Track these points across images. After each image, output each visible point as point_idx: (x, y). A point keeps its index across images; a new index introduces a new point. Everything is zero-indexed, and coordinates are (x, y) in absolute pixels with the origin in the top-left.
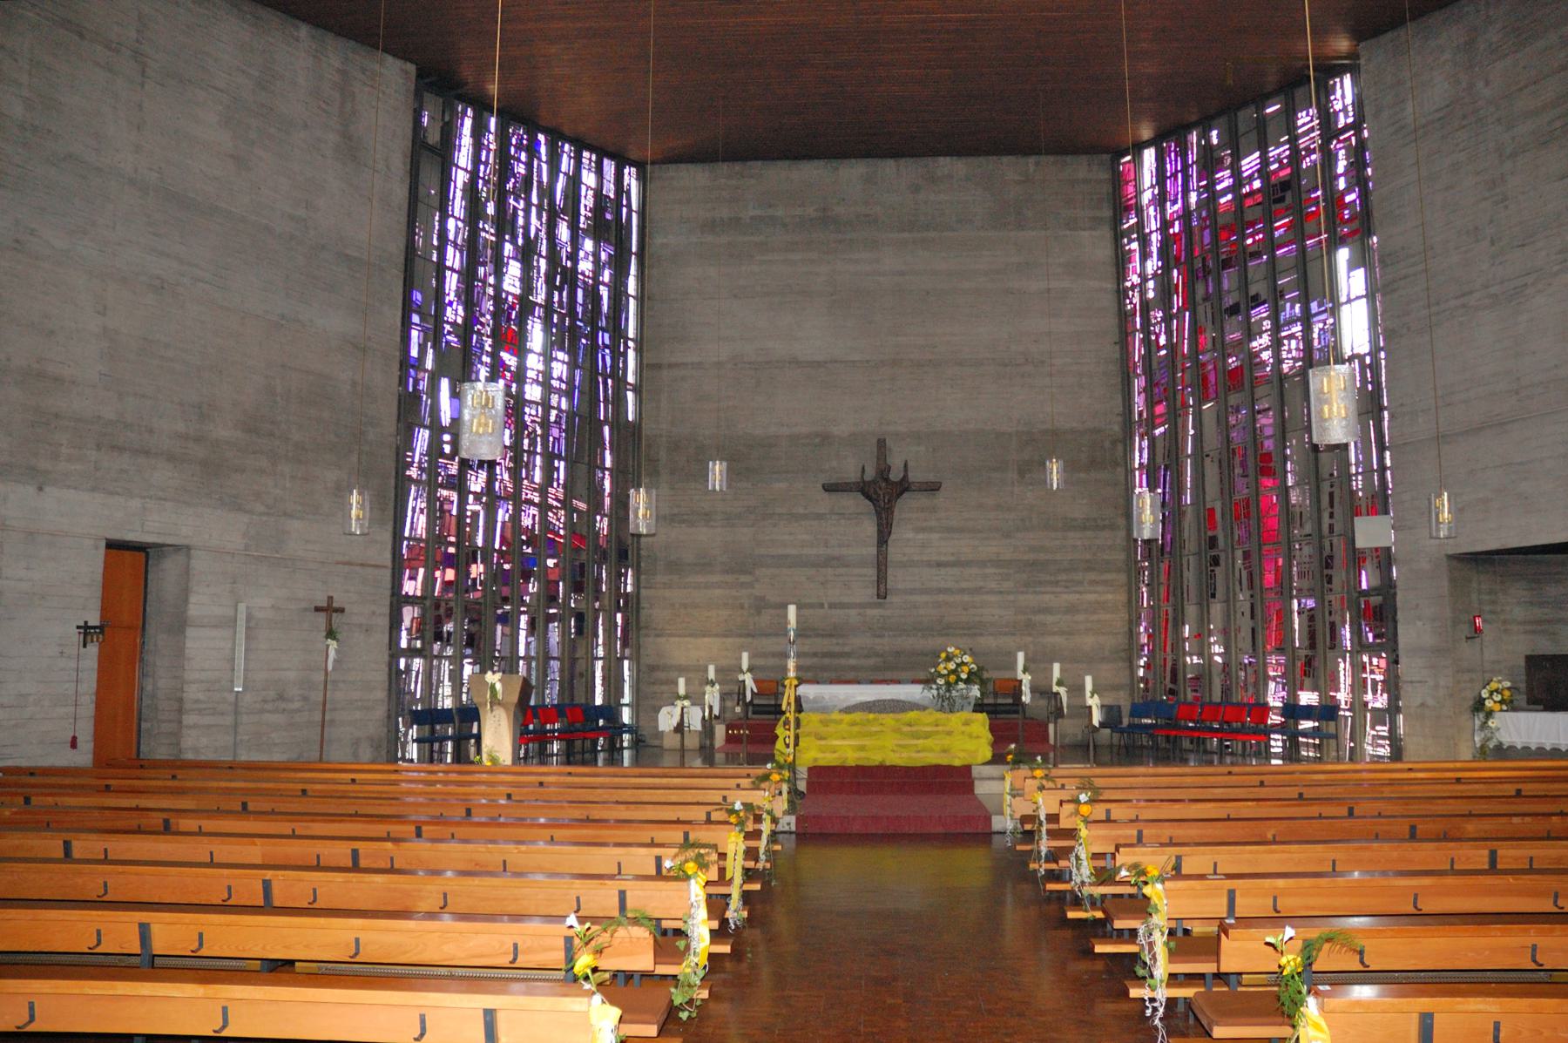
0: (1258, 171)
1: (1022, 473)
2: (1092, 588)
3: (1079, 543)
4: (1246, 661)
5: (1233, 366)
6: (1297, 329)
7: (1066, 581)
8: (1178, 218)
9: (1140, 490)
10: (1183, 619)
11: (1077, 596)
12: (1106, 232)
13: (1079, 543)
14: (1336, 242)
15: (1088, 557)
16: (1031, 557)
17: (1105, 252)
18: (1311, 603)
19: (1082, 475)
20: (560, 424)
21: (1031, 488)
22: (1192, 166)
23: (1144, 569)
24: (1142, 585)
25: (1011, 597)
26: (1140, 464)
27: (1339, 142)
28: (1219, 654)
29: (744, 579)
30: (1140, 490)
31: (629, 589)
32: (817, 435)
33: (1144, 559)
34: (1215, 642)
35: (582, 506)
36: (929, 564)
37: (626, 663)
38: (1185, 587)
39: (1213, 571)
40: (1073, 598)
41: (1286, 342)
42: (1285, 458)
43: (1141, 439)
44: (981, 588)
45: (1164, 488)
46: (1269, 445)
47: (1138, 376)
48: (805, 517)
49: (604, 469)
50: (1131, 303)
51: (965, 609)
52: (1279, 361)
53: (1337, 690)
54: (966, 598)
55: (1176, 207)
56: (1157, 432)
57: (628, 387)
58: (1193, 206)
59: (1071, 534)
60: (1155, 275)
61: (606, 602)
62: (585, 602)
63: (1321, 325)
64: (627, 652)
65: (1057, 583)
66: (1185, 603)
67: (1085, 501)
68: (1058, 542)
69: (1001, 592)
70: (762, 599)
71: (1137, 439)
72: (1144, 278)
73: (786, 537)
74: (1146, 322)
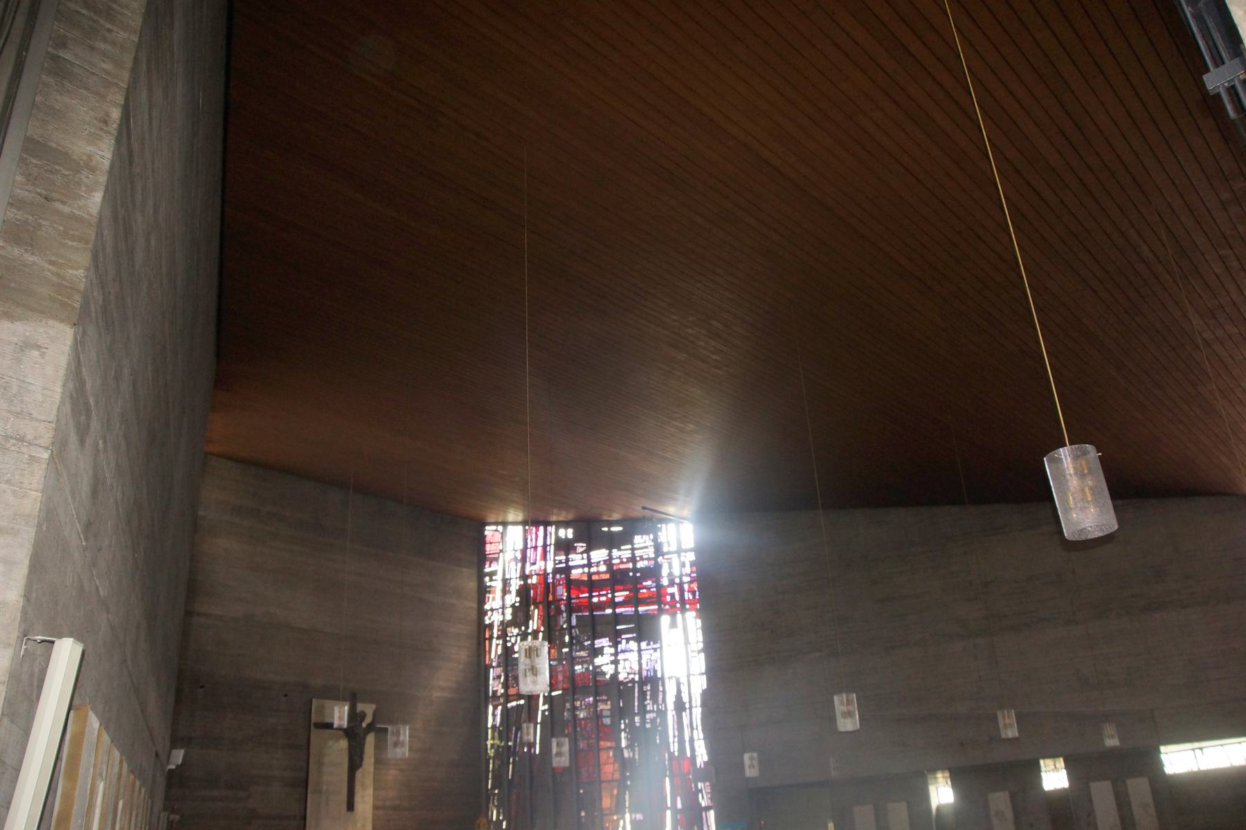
5: (578, 671)
6: (633, 656)
9: (492, 742)
12: (474, 571)
14: (661, 611)
17: (472, 585)
18: (639, 816)
23: (495, 794)
24: (491, 805)
26: (494, 727)
27: (664, 558)
30: (492, 742)
33: (494, 787)
41: (621, 662)
43: (495, 708)
47: (493, 667)
52: (616, 673)
55: (534, 568)
58: (549, 570)
60: (513, 606)
63: (649, 657)
71: (491, 708)
72: (503, 607)
74: (503, 635)
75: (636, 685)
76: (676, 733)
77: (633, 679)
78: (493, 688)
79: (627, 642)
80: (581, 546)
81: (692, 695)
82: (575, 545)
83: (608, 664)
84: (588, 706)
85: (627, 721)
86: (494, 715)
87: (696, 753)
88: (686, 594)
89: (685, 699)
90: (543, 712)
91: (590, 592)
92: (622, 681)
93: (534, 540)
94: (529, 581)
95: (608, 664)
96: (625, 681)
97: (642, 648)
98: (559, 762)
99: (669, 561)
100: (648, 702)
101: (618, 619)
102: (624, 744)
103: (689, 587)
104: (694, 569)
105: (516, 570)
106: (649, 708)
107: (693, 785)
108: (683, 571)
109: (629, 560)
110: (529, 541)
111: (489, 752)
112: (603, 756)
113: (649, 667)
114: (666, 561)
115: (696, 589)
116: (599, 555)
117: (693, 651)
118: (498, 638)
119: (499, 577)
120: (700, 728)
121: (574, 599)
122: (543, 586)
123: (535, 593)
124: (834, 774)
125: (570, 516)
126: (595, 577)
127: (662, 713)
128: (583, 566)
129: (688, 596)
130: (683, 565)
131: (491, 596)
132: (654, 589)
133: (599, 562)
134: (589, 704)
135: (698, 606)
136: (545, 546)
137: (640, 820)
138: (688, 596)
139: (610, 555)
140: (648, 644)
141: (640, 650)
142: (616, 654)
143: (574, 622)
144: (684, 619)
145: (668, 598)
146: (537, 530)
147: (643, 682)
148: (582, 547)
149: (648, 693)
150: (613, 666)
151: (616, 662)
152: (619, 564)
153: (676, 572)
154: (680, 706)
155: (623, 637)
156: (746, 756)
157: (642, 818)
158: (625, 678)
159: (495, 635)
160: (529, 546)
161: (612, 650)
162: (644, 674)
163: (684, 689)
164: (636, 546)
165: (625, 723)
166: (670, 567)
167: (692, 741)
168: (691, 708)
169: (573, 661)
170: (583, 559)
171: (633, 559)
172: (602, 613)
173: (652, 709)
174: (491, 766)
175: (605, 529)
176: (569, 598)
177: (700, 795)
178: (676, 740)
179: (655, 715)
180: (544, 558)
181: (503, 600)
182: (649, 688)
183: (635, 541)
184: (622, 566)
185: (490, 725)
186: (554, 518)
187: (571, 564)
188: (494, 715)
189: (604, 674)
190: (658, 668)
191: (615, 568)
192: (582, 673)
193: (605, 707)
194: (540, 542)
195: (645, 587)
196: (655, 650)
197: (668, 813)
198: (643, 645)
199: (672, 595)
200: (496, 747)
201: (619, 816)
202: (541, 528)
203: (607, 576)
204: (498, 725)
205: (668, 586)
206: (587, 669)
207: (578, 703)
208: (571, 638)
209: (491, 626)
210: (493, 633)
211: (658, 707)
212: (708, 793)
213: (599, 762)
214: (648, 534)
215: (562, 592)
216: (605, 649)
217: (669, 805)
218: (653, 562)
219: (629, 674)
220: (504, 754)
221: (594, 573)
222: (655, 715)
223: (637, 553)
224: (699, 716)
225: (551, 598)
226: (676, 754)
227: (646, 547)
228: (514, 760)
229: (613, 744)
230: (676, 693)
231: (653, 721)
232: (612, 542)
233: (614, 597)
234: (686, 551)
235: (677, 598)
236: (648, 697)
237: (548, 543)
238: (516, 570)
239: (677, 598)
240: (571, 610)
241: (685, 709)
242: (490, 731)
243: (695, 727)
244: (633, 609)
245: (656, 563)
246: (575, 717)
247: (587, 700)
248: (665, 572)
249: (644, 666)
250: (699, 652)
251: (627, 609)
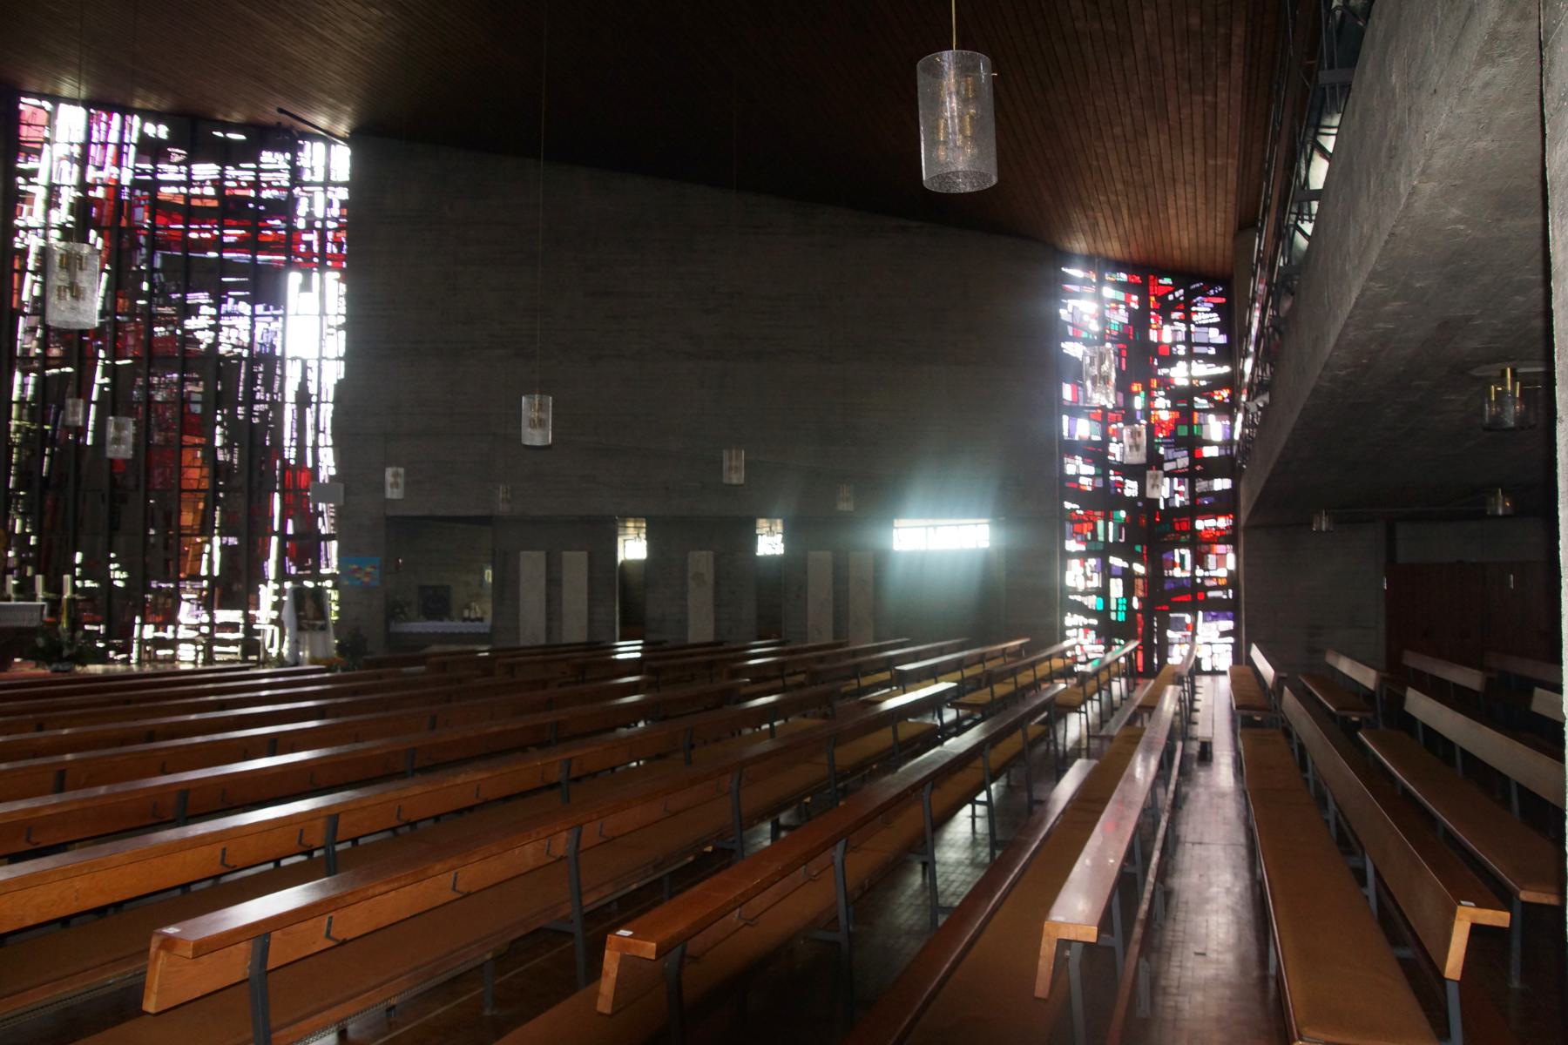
0: (213, 181)
5: (159, 334)
6: (243, 322)
8: (104, 185)
9: (17, 422)
14: (290, 265)
18: (233, 541)
22: (128, 145)
24: (12, 512)
26: (22, 401)
27: (303, 191)
30: (17, 422)
33: (18, 487)
34: (116, 570)
41: (224, 328)
42: (216, 424)
43: (25, 374)
46: (197, 409)
47: (25, 315)
50: (22, 243)
53: (257, 608)
55: (100, 174)
56: (48, 372)
63: (266, 326)
75: (243, 363)
76: (295, 435)
77: (240, 354)
79: (236, 303)
80: (177, 154)
81: (323, 386)
82: (169, 150)
83: (203, 329)
84: (167, 386)
85: (225, 412)
87: (320, 464)
88: (329, 245)
89: (313, 389)
90: (102, 386)
91: (187, 223)
92: (223, 355)
93: (103, 133)
94: (91, 193)
95: (203, 329)
96: (227, 355)
97: (257, 312)
98: (117, 451)
99: (309, 195)
100: (259, 387)
101: (224, 267)
102: (218, 442)
103: (335, 236)
104: (345, 212)
105: (71, 173)
106: (259, 396)
107: (311, 506)
108: (328, 213)
109: (251, 185)
110: (95, 133)
112: (187, 457)
113: (265, 340)
114: (304, 194)
115: (343, 240)
116: (205, 171)
117: (330, 327)
118: (34, 273)
119: (42, 179)
120: (329, 431)
121: (160, 229)
122: (112, 203)
123: (100, 214)
124: (503, 508)
125: (165, 105)
126: (196, 202)
127: (277, 407)
128: (178, 184)
129: (331, 248)
130: (329, 204)
131: (26, 207)
132: (283, 232)
133: (204, 181)
134: (171, 381)
135: (344, 265)
136: (120, 145)
137: (234, 546)
138: (331, 248)
139: (222, 174)
140: (267, 309)
141: (253, 316)
142: (217, 317)
143: (158, 263)
144: (322, 281)
145: (303, 248)
146: (110, 118)
147: (253, 360)
148: (180, 154)
149: (260, 376)
150: (212, 334)
151: (216, 329)
152: (233, 188)
153: (319, 212)
154: (303, 399)
155: (230, 293)
156: (389, 472)
157: (236, 543)
158: (229, 352)
159: (31, 267)
160: (94, 140)
161: (213, 311)
162: (257, 348)
163: (312, 375)
164: (262, 166)
165: (222, 414)
166: (311, 205)
167: (316, 447)
168: (318, 403)
169: (152, 319)
170: (180, 173)
171: (256, 185)
172: (202, 255)
173: (262, 398)
175: (219, 134)
176: (153, 227)
177: (320, 519)
178: (294, 444)
179: (266, 407)
180: (118, 163)
181: (47, 215)
182: (261, 369)
183: (262, 159)
184: (239, 192)
185: (15, 397)
186: (138, 104)
187: (160, 177)
189: (199, 342)
190: (278, 342)
191: (227, 192)
192: (164, 338)
193: (195, 389)
194: (114, 137)
195: (270, 228)
196: (276, 317)
197: (274, 540)
198: (260, 309)
199: (309, 244)
200: (23, 430)
201: (205, 538)
202: (117, 117)
203: (215, 204)
204: (28, 399)
205: (304, 231)
206: (173, 332)
207: (155, 380)
208: (152, 286)
209: (24, 253)
210: (26, 263)
211: (272, 397)
212: (332, 517)
213: (181, 462)
214: (283, 151)
215: (143, 217)
216: (202, 308)
217: (276, 528)
218: (285, 193)
219: (234, 346)
220: (35, 442)
221: (196, 197)
222: (266, 407)
223: (264, 177)
224: (329, 415)
225: (124, 223)
226: (292, 462)
227: (278, 171)
228: (52, 451)
229: (203, 440)
230: (299, 380)
231: (263, 414)
232: (227, 155)
233: (223, 235)
234: (336, 185)
235: (316, 249)
236: (259, 382)
237: (126, 140)
238: (71, 173)
239: (316, 249)
240: (154, 245)
241: (309, 404)
242: (15, 407)
243: (322, 429)
244: (249, 256)
245: (291, 195)
246: (149, 400)
247: (168, 376)
248: (302, 209)
249: (258, 338)
250: (339, 328)
251: (239, 255)
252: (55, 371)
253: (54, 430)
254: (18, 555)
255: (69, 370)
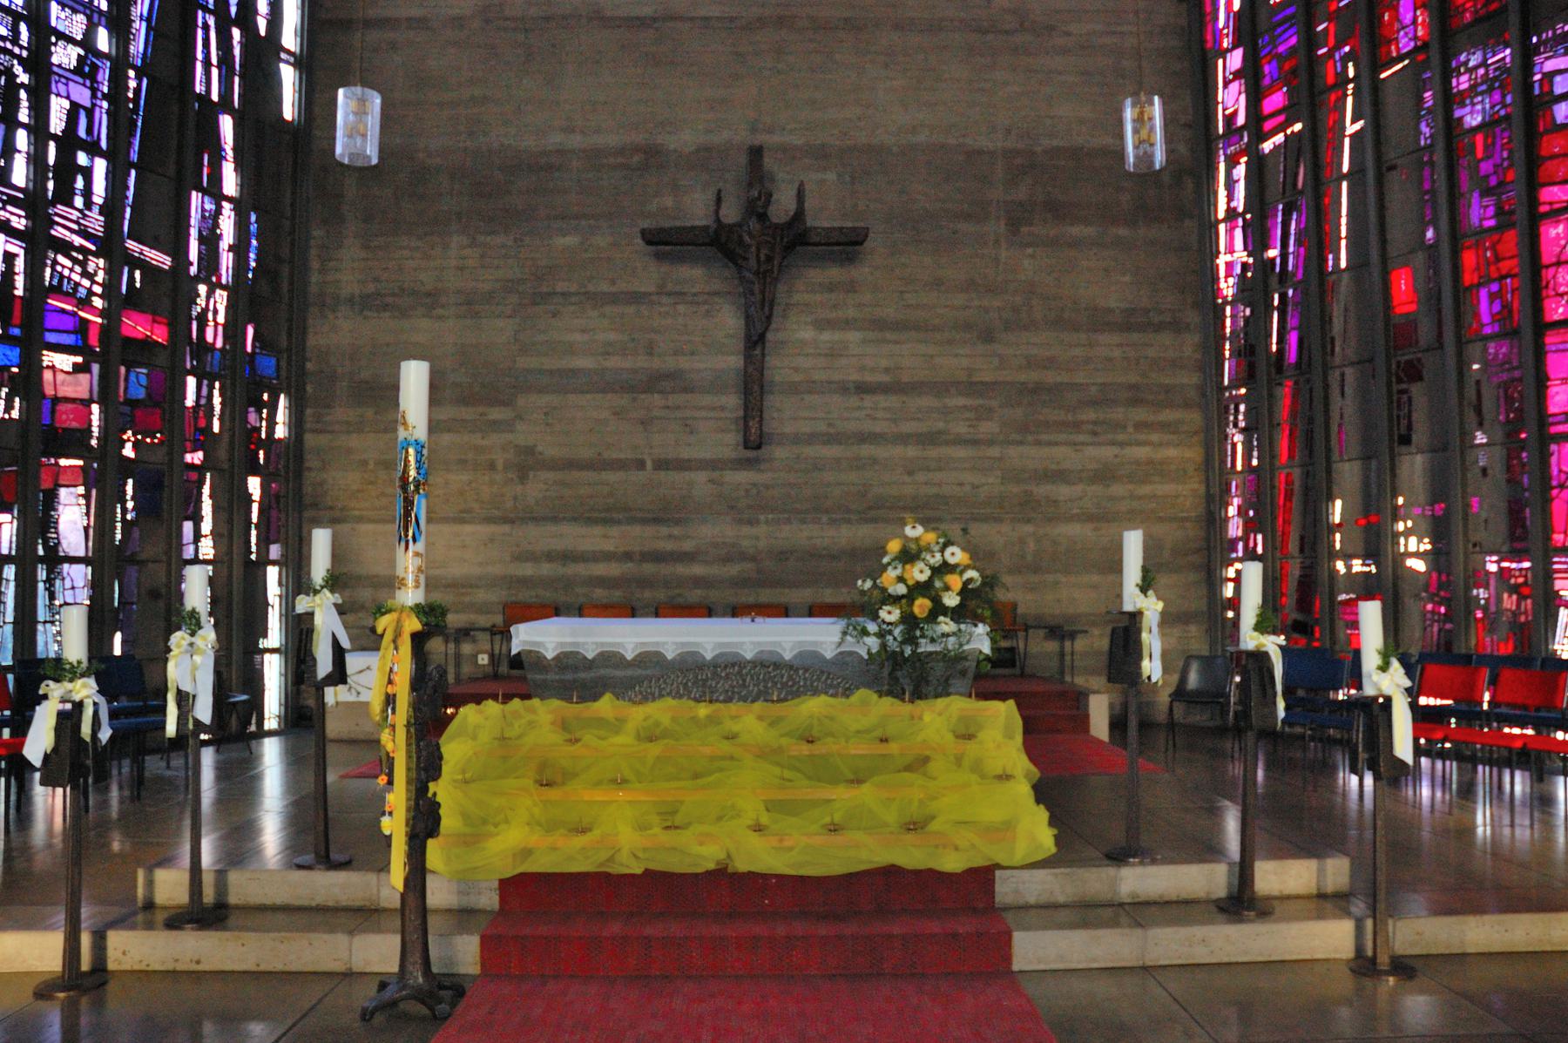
1: (1014, 224)
2: (1142, 437)
3: (1117, 353)
4: (1493, 568)
7: (1095, 423)
9: (1228, 258)
10: (1329, 489)
11: (1115, 450)
13: (1117, 353)
15: (1133, 378)
16: (1033, 376)
19: (1123, 232)
20: (94, 79)
21: (1030, 251)
24: (1231, 430)
25: (994, 452)
26: (1231, 213)
28: (1417, 555)
29: (496, 414)
30: (1228, 258)
31: (281, 432)
32: (637, 149)
33: (1235, 384)
35: (162, 260)
36: (843, 389)
37: (272, 573)
38: (1334, 428)
39: (1401, 392)
40: (1107, 453)
43: (1232, 162)
44: (940, 432)
45: (1285, 245)
48: (614, 299)
49: (217, 195)
51: (910, 473)
54: (912, 451)
56: (1267, 146)
57: (283, 56)
59: (1104, 338)
61: (222, 453)
62: (164, 449)
64: (275, 551)
65: (1077, 426)
66: (1335, 456)
67: (1127, 278)
68: (1077, 351)
69: (975, 442)
70: (530, 451)
71: (1222, 167)
73: (578, 337)
78: (1224, 110)
86: (1230, 185)
111: (1223, 285)
174: (1228, 322)
188: (1230, 185)
200: (1238, 270)
228: (1283, 297)
252: (1279, 138)
253: (1284, 255)
254: (1241, 512)
255: (1298, 127)
